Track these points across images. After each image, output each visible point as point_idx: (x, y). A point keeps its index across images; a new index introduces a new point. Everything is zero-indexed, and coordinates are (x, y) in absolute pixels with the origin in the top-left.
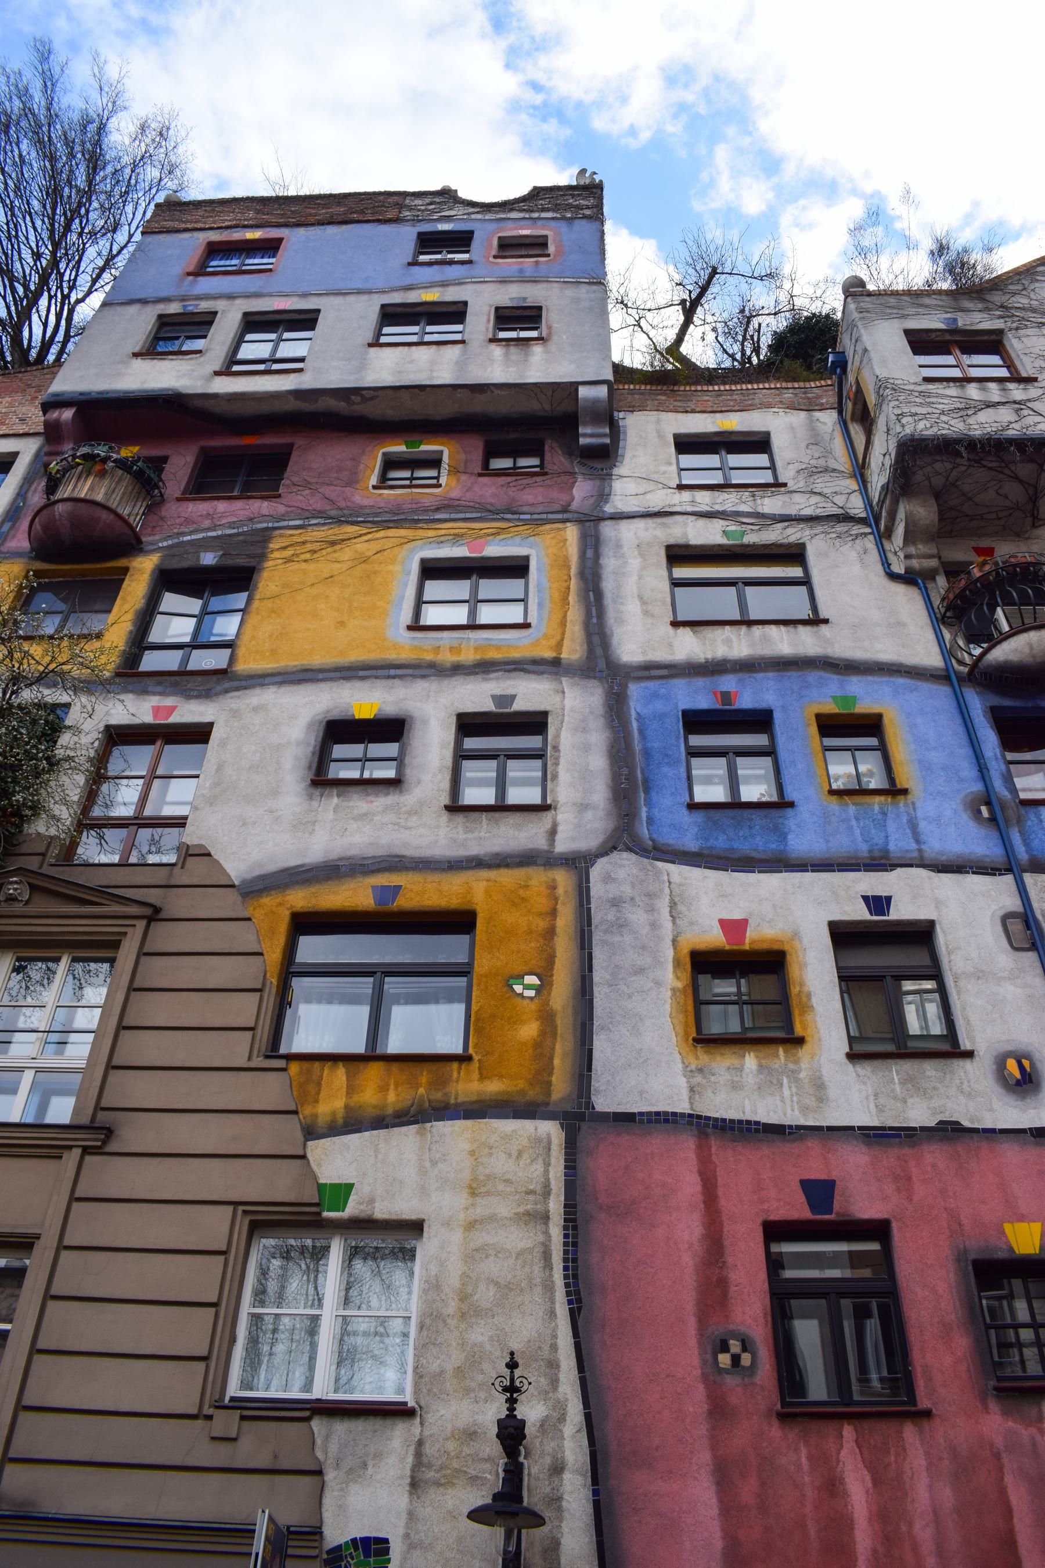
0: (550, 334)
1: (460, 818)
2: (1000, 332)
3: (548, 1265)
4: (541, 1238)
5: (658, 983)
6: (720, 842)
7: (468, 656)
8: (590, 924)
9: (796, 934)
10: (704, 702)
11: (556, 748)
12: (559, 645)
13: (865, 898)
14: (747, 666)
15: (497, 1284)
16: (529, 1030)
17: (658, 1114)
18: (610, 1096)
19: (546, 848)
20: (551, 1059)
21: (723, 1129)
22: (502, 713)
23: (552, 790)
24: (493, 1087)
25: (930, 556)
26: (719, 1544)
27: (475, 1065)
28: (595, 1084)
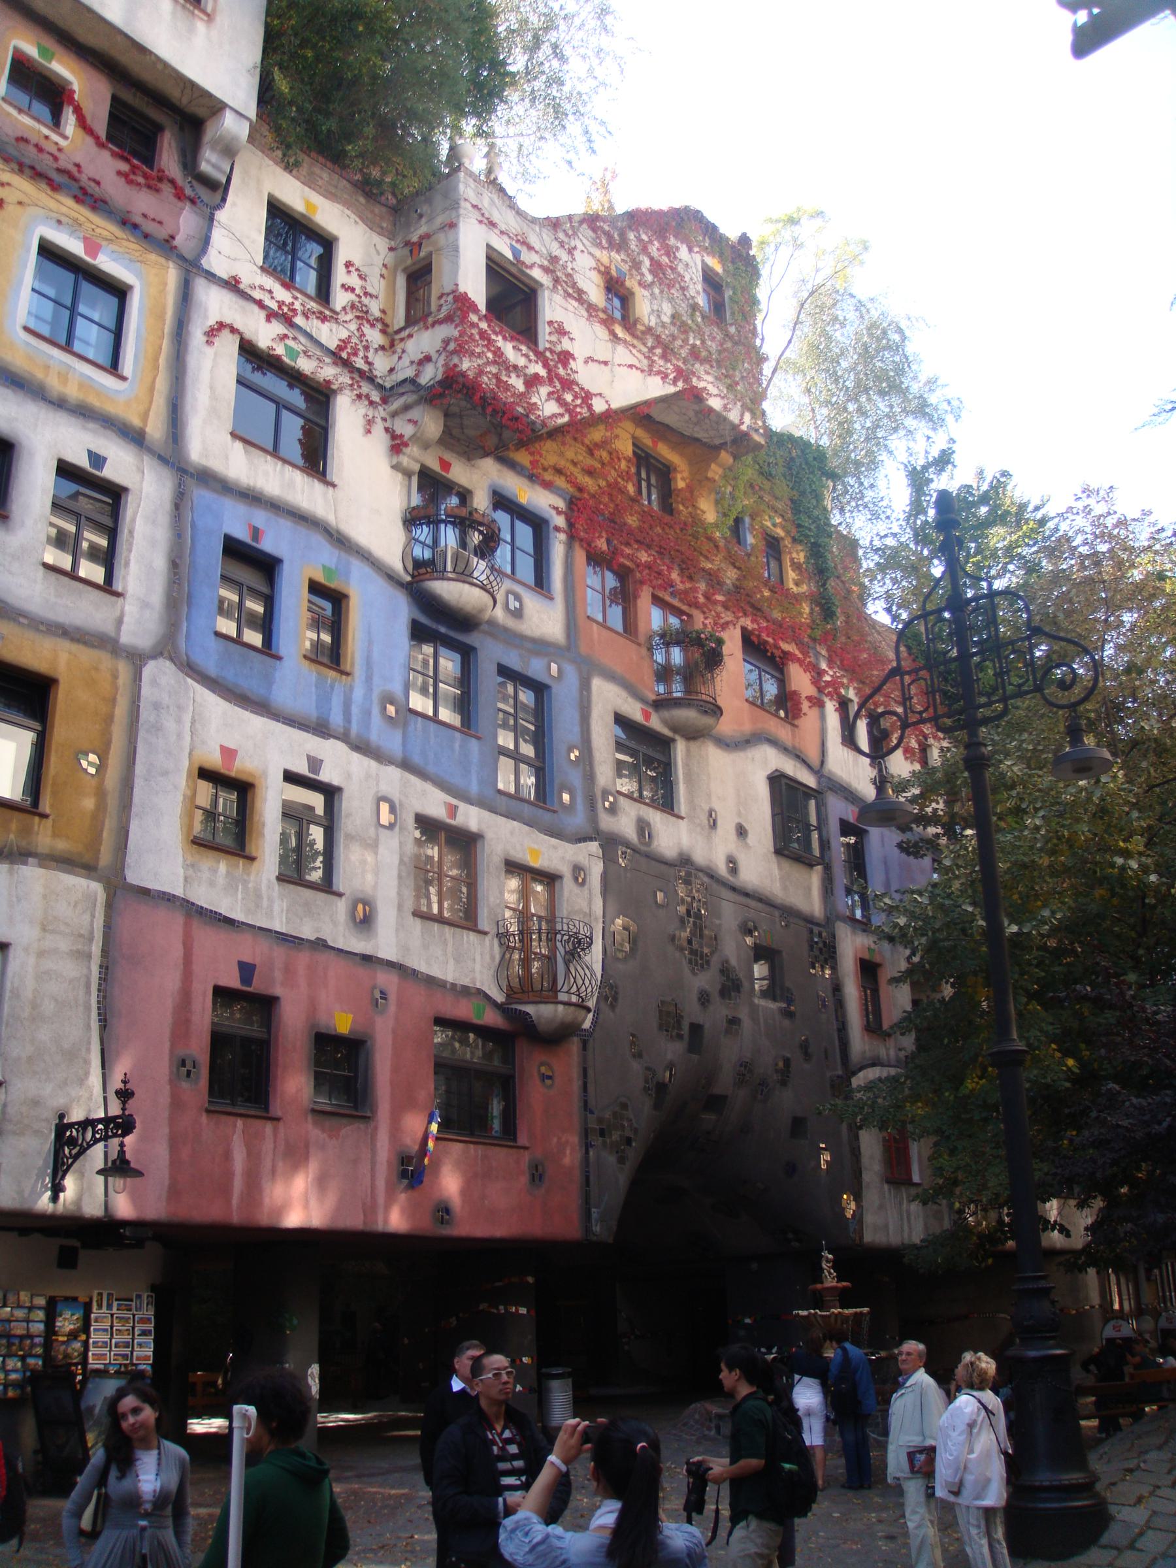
0: (214, 10)
1: (53, 576)
2: (542, 285)
3: (88, 992)
4: (85, 971)
5: (175, 787)
6: (230, 675)
7: (72, 392)
8: (138, 722)
9: (265, 773)
10: (241, 533)
11: (131, 532)
12: (145, 416)
13: (309, 757)
14: (276, 507)
15: (56, 1000)
16: (89, 803)
17: (164, 893)
18: (137, 875)
19: (113, 634)
20: (102, 831)
21: (201, 914)
22: (93, 475)
23: (124, 578)
24: (62, 845)
25: (417, 461)
26: (167, 1183)
27: (49, 822)
28: (130, 860)
